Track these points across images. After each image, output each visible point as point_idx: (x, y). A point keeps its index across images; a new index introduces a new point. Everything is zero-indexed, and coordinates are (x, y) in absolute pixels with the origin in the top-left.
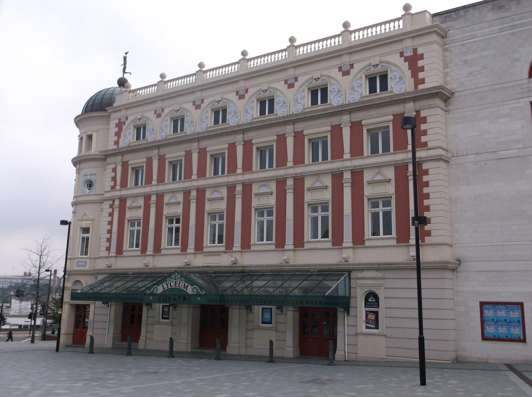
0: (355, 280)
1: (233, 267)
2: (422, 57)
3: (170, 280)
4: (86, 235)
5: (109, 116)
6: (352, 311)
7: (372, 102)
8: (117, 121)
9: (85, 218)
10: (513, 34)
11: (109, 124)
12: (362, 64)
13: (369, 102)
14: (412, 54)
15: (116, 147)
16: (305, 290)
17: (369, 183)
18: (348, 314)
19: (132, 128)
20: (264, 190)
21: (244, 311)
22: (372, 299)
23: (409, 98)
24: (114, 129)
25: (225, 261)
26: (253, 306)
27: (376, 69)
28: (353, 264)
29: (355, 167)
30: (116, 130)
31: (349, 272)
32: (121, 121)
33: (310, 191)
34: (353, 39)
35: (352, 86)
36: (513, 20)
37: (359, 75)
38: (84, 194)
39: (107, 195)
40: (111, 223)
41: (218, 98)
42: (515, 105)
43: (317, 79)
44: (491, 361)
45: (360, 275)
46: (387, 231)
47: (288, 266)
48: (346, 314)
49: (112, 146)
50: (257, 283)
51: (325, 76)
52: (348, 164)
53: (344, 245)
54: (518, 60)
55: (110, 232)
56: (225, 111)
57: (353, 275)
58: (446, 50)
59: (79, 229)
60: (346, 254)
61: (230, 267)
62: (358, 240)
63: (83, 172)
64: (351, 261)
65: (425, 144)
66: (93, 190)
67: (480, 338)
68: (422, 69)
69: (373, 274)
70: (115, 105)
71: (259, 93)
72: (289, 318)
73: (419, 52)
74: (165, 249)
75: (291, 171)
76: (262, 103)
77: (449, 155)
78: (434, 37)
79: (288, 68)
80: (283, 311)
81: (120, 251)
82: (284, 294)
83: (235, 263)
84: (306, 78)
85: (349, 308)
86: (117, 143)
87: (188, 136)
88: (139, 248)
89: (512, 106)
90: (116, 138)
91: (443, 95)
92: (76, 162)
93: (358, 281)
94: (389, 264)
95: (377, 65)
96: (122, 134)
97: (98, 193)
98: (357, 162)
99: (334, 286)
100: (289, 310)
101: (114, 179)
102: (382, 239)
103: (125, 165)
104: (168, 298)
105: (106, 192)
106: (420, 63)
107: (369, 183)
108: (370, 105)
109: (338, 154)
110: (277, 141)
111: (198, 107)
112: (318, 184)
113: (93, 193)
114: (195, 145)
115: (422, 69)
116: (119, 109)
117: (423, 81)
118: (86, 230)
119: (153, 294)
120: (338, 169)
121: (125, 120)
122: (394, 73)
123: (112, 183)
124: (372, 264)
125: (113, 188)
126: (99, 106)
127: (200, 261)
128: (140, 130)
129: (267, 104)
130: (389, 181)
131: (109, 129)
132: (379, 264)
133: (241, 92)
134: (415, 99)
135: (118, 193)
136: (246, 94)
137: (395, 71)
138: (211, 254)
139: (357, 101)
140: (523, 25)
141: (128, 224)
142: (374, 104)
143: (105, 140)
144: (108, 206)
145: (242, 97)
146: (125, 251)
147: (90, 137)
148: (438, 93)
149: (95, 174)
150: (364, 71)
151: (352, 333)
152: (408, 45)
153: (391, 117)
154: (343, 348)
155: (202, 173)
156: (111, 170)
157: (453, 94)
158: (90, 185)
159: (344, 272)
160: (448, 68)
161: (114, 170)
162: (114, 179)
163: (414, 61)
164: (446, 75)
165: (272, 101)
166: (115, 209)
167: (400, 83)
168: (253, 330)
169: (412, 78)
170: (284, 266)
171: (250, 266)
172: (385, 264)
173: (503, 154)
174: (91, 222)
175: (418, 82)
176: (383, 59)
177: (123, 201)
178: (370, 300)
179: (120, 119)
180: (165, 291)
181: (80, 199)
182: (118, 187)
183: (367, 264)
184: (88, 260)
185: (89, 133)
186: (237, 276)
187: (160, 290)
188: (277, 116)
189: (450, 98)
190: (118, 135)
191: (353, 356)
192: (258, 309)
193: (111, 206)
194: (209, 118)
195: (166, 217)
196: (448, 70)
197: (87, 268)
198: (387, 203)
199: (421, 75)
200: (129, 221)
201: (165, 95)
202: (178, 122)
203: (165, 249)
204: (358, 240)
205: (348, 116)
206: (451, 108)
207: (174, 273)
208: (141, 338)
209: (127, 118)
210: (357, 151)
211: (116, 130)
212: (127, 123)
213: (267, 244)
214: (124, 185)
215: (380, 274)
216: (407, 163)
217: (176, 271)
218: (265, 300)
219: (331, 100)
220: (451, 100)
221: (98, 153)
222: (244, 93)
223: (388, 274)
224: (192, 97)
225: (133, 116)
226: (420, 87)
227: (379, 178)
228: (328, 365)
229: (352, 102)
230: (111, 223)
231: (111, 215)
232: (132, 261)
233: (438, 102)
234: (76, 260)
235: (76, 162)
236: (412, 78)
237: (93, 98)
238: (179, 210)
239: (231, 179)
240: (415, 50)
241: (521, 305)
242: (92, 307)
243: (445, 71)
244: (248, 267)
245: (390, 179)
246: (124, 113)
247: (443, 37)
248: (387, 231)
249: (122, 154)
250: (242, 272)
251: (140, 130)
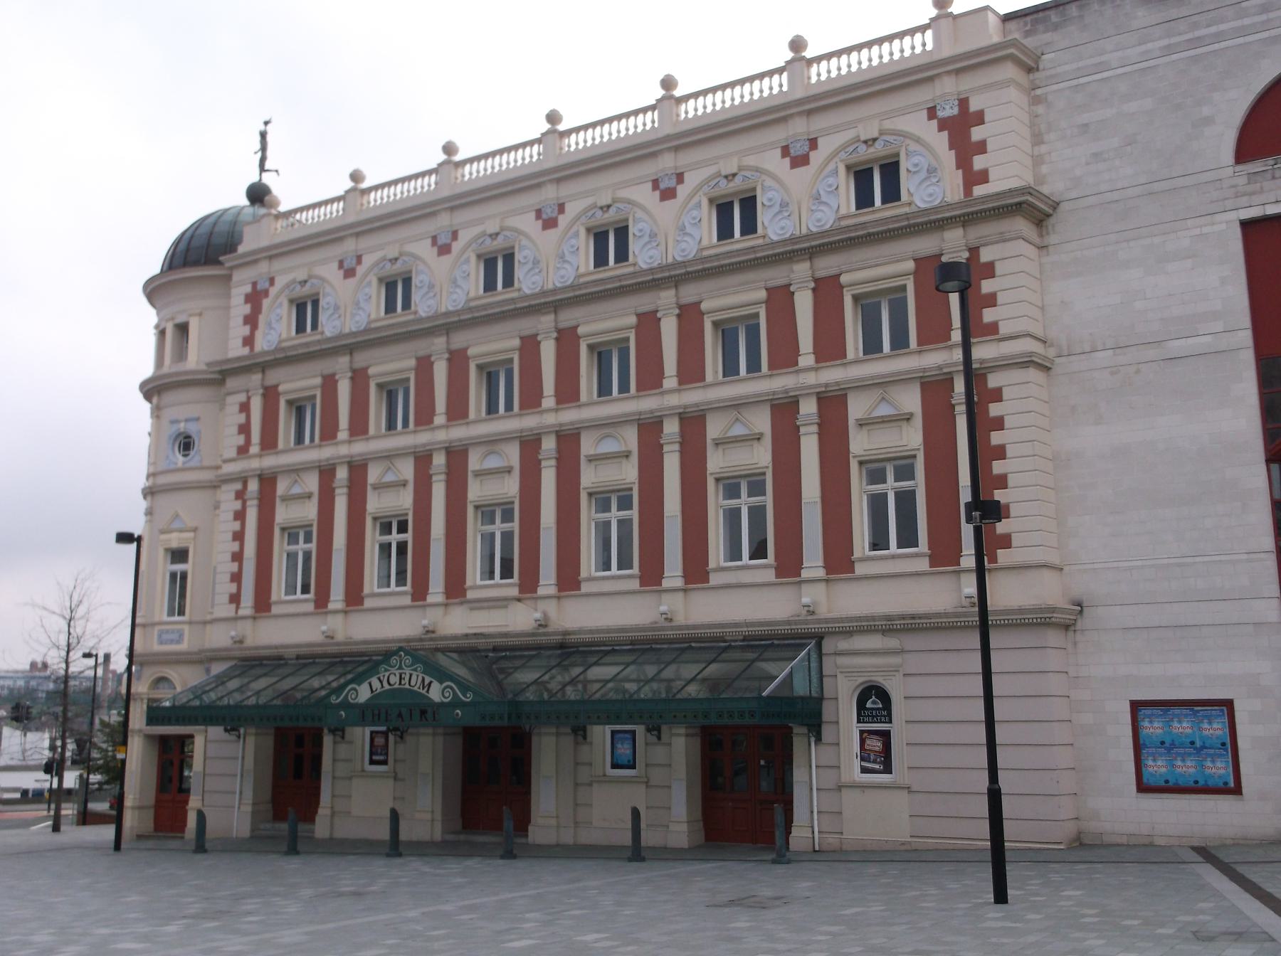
0: (832, 658)
1: (540, 635)
2: (979, 118)
3: (386, 670)
4: (179, 567)
5: (228, 278)
6: (827, 731)
7: (863, 229)
8: (248, 289)
9: (176, 525)
10: (1195, 59)
11: (229, 296)
12: (838, 139)
13: (856, 230)
14: (956, 111)
15: (246, 351)
16: (714, 684)
17: (861, 424)
18: (819, 739)
19: (286, 303)
20: (609, 447)
21: (568, 741)
22: (874, 702)
23: (951, 218)
24: (240, 309)
25: (518, 620)
26: (589, 727)
27: (871, 150)
28: (827, 621)
29: (827, 385)
30: (247, 309)
31: (819, 638)
32: (259, 287)
33: (721, 448)
35: (814, 191)
36: (1196, 26)
37: (831, 166)
38: (172, 467)
39: (229, 469)
40: (239, 536)
41: (492, 227)
42: (1205, 230)
43: (731, 177)
44: (1159, 841)
45: (843, 645)
46: (907, 539)
47: (672, 628)
48: (813, 739)
49: (236, 350)
50: (597, 672)
51: (749, 168)
52: (811, 379)
53: (805, 574)
54: (1209, 121)
55: (238, 557)
56: (509, 259)
57: (828, 645)
58: (1036, 101)
59: (161, 552)
60: (809, 595)
61: (533, 635)
62: (839, 561)
63: (169, 413)
64: (823, 612)
65: (993, 328)
66: (195, 458)
67: (1134, 788)
68: (981, 147)
69: (875, 642)
70: (241, 249)
71: (590, 214)
72: (677, 753)
73: (974, 106)
74: (374, 595)
75: (674, 400)
76: (600, 238)
77: (1051, 353)
78: (1009, 71)
79: (661, 151)
80: (663, 736)
81: (263, 603)
82: (664, 696)
83: (542, 625)
84: (701, 174)
85: (820, 726)
86: (249, 341)
87: (421, 320)
88: (311, 596)
89: (1197, 231)
90: (246, 330)
91: (1032, 210)
92: (151, 390)
93: (842, 661)
94: (913, 617)
95: (875, 140)
96: (262, 319)
97: (206, 463)
98: (833, 375)
99: (782, 673)
100: (679, 735)
101: (245, 429)
102: (893, 557)
103: (270, 394)
104: (383, 716)
105: (225, 461)
106: (977, 134)
107: (861, 424)
108: (858, 237)
109: (785, 357)
110: (638, 328)
111: (444, 250)
112: (738, 430)
113: (192, 464)
114: (440, 342)
115: (981, 147)
116: (253, 259)
117: (983, 177)
118: (179, 555)
119: (346, 705)
120: (786, 391)
121: (267, 284)
122: (916, 159)
123: (241, 440)
124: (873, 618)
125: (243, 450)
126: (203, 253)
127: (458, 623)
128: (305, 309)
129: (610, 239)
130: (908, 418)
131: (228, 308)
132: (889, 618)
133: (549, 211)
134: (967, 220)
135: (255, 464)
136: (561, 218)
137: (915, 153)
138: (486, 604)
139: (827, 227)
140: (1218, 37)
141: (282, 536)
142: (869, 235)
143: (219, 334)
144: (232, 495)
145: (550, 224)
146: (276, 603)
147: (183, 329)
148: (1020, 204)
149: (198, 419)
150: (843, 155)
151: (829, 784)
152: (946, 92)
153: (911, 265)
154: (808, 820)
155: (457, 411)
156: (237, 408)
157: (1056, 206)
158: (186, 444)
159: (806, 640)
160: (1043, 143)
161: (245, 408)
162: (245, 429)
163: (961, 128)
164: (1037, 161)
165: (622, 233)
166: (249, 503)
167: (930, 183)
168: (590, 785)
169: (958, 168)
170: (663, 629)
171: (580, 631)
172: (903, 617)
173: (1177, 347)
174: (191, 535)
175: (974, 178)
176: (888, 125)
177: (268, 481)
178: (869, 705)
179: (254, 284)
180: (376, 697)
181: (162, 480)
182: (254, 449)
183: (859, 619)
184: (186, 628)
185: (181, 319)
186: (549, 657)
187: (363, 694)
188: (637, 268)
189: (1049, 216)
190: (251, 321)
191: (832, 840)
192: (601, 734)
193: (240, 495)
194: (473, 276)
195: (375, 519)
196: (1043, 149)
197: (183, 647)
198: (905, 472)
199: (979, 162)
200: (283, 529)
201: (363, 223)
202: (397, 288)
203: (374, 595)
204: (839, 561)
205: (807, 265)
206: (1052, 239)
207: (395, 653)
208: (320, 811)
210: (830, 347)
211: (247, 309)
212: (273, 291)
213: (620, 577)
214: (269, 443)
215: (892, 642)
216: (950, 373)
217: (401, 649)
218: (618, 710)
219: (765, 228)
220: (1052, 220)
221: (204, 367)
222: (554, 215)
223: (911, 642)
224: (430, 226)
225: (288, 274)
226: (979, 191)
227: (884, 410)
228: (774, 862)
229: (814, 230)
230: (239, 536)
231: (240, 516)
232: (294, 627)
233: (1021, 225)
234: (157, 628)
235: (151, 390)
236: (958, 168)
237: (188, 235)
238: (404, 501)
239: (530, 422)
240: (963, 103)
241: (1228, 704)
242: (199, 742)
243: (1037, 150)
244: (574, 633)
245: (911, 415)
246: (263, 267)
247: (1030, 70)
248: (907, 539)
249: (263, 367)
250: (562, 646)
251: (305, 309)
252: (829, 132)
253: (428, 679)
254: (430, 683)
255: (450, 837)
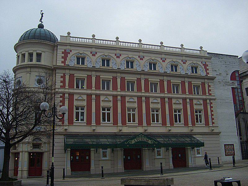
15: (63, 65)
20: (155, 101)
24: (60, 55)
32: (67, 51)
34: (71, 40)
49: (59, 63)
62: (98, 123)
72: (120, 154)
90: (63, 60)
91: (212, 79)
101: (64, 82)
102: (106, 123)
103: (72, 76)
123: (62, 84)
125: (63, 87)
147: (39, 55)
151: (195, 158)
154: (191, 164)
159: (189, 135)
161: (64, 77)
162: (64, 82)
167: (201, 72)
173: (227, 101)
190: (65, 58)
207: (138, 135)
208: (91, 168)
209: (71, 51)
213: (81, 123)
214: (71, 86)
226: (208, 75)
237: (28, 32)
241: (233, 145)
242: (161, 151)
246: (68, 47)
252: (123, 54)
253: (148, 139)
254: (148, 140)
255: (126, 171)
